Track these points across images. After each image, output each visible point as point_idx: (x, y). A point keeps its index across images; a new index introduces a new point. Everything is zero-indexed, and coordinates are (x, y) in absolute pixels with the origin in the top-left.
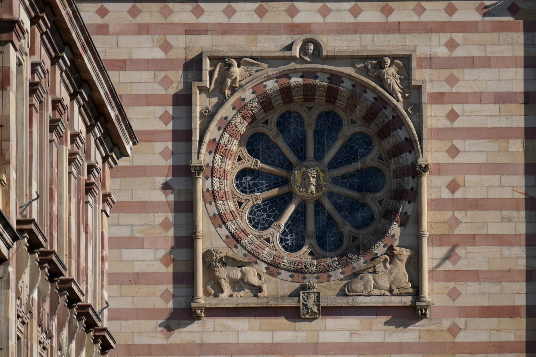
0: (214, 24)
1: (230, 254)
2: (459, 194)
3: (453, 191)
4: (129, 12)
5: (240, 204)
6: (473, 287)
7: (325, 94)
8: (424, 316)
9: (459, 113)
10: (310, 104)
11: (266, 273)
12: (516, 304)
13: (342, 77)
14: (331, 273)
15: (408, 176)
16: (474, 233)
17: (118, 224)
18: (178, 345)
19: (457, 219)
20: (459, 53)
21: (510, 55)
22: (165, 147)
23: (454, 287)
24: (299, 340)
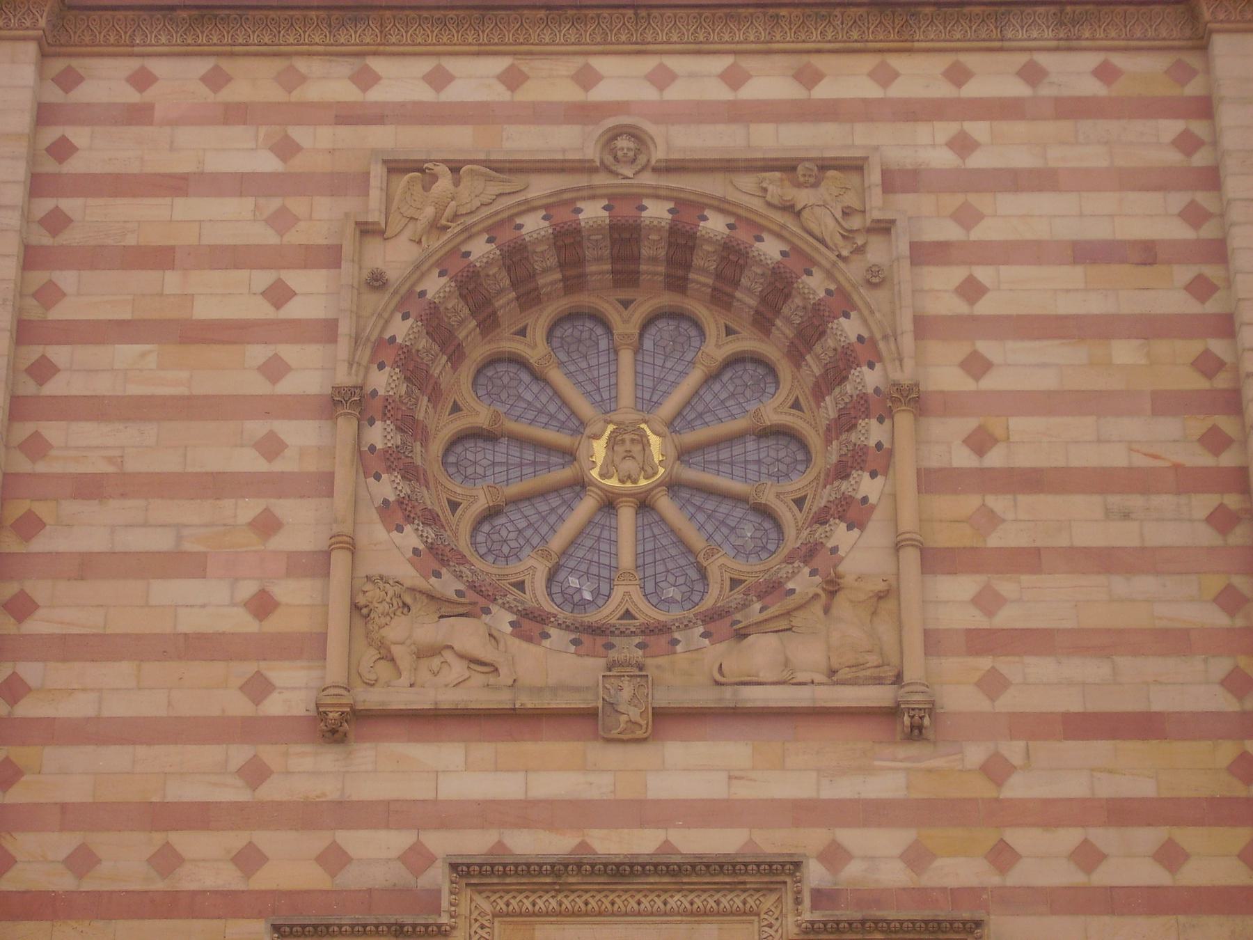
0: (403, 105)
1: (420, 583)
2: (995, 458)
3: (980, 451)
4: (205, 79)
5: (454, 506)
6: (1040, 668)
7: (662, 253)
8: (916, 733)
9: (988, 285)
10: (624, 294)
11: (512, 634)
12: (1156, 707)
13: (704, 206)
14: (677, 635)
15: (868, 416)
16: (1038, 544)
17: (145, 525)
18: (280, 803)
19: (992, 511)
20: (977, 160)
21: (1104, 163)
22: (271, 354)
23: (993, 668)
24: (594, 794)
